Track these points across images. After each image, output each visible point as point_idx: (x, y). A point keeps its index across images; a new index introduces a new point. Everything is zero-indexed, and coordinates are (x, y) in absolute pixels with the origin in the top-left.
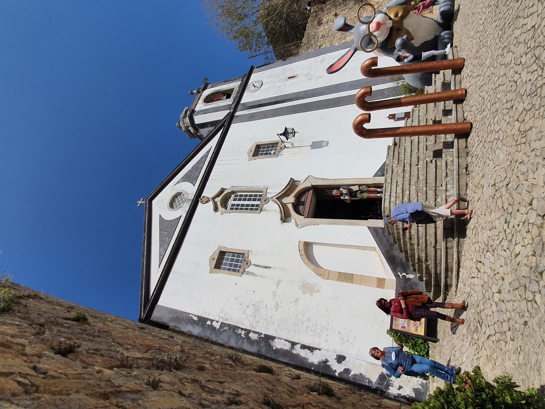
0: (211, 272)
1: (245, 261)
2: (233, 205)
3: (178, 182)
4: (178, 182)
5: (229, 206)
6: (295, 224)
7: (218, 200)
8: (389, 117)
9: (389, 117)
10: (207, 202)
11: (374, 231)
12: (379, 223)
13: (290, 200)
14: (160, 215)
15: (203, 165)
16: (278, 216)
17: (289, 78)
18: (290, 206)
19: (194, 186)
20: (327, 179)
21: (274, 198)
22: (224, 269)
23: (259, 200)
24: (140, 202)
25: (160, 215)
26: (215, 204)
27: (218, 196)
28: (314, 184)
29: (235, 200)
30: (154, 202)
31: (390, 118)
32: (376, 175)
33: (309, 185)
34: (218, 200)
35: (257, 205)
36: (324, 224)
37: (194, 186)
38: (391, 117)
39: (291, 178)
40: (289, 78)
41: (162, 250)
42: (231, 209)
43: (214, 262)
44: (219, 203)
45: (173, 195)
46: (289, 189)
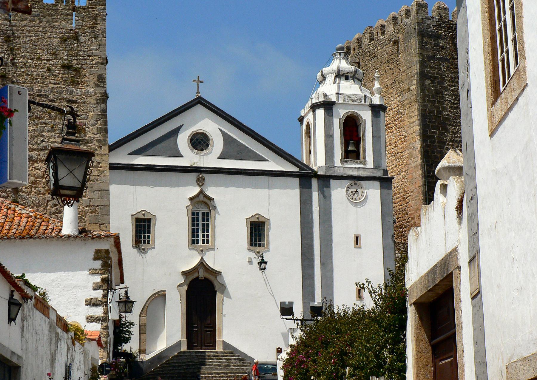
2: (197, 214)
8: (279, 348)
9: (279, 348)
11: (179, 344)
12: (184, 348)
13: (202, 274)
14: (183, 125)
17: (357, 238)
18: (196, 275)
19: (218, 158)
25: (183, 125)
26: (198, 195)
27: (206, 196)
29: (203, 214)
30: (199, 105)
31: (277, 349)
32: (223, 341)
37: (218, 158)
38: (279, 349)
39: (221, 272)
40: (357, 238)
44: (197, 199)
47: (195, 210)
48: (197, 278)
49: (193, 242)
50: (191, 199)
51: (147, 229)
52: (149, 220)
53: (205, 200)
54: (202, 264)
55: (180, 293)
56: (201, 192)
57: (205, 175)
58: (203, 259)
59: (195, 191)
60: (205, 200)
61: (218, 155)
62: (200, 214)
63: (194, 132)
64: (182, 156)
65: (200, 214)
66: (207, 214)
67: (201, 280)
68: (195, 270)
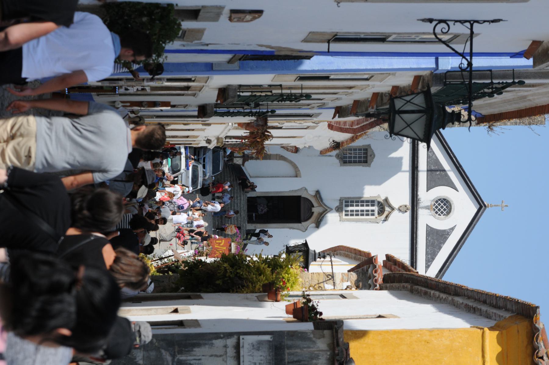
0: (369, 146)
1: (341, 158)
2: (373, 205)
3: (452, 229)
4: (452, 229)
5: (376, 203)
6: (308, 190)
7: (387, 209)
13: (316, 210)
14: (457, 191)
15: (427, 250)
16: (323, 195)
18: (315, 204)
19: (427, 225)
20: (290, 228)
21: (329, 210)
22: (360, 150)
25: (457, 191)
26: (390, 206)
28: (300, 224)
29: (373, 211)
33: (303, 223)
36: (286, 192)
37: (427, 225)
41: (434, 157)
43: (369, 154)
45: (451, 214)
46: (319, 218)
47: (376, 203)
48: (313, 206)
50: (386, 200)
52: (366, 162)
53: (386, 213)
54: (326, 210)
55: (298, 190)
56: (393, 209)
59: (395, 204)
63: (451, 203)
64: (427, 191)
66: (373, 215)
67: (311, 210)
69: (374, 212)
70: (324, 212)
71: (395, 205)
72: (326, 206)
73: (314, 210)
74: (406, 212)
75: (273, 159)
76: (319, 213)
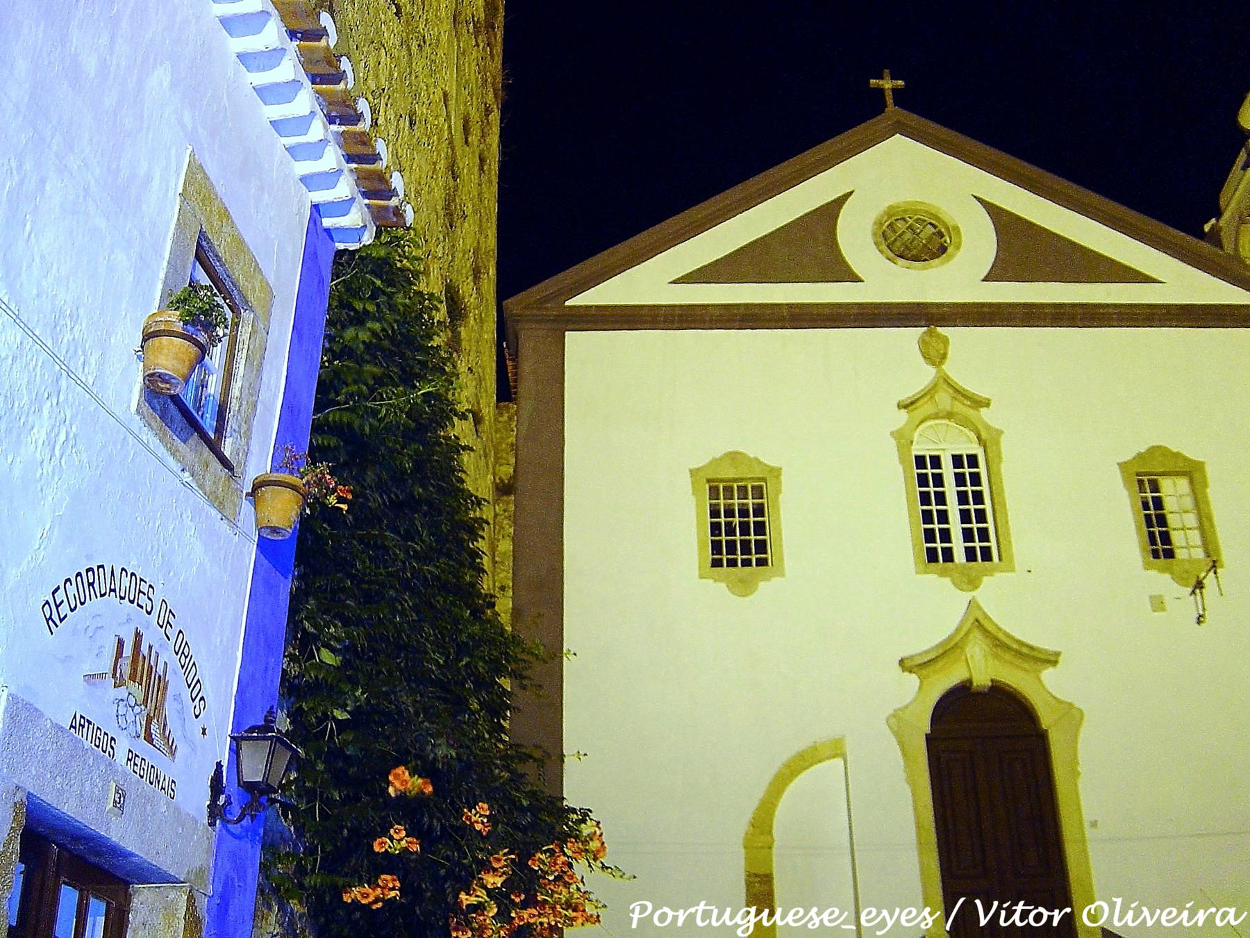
2: (936, 461)
10: (927, 357)
19: (983, 280)
20: (1074, 774)
23: (970, 555)
24: (887, 84)
26: (930, 392)
27: (959, 393)
29: (957, 461)
34: (944, 399)
35: (948, 555)
42: (920, 461)
43: (728, 473)
49: (932, 556)
50: (906, 406)
51: (752, 519)
55: (901, 743)
57: (951, 333)
58: (980, 608)
60: (960, 408)
61: (982, 277)
62: (947, 464)
64: (863, 281)
65: (947, 464)
68: (949, 650)
69: (961, 456)
70: (985, 632)
71: (923, 375)
72: (962, 622)
73: (982, 679)
74: (945, 341)
75: (768, 861)
76: (996, 656)
